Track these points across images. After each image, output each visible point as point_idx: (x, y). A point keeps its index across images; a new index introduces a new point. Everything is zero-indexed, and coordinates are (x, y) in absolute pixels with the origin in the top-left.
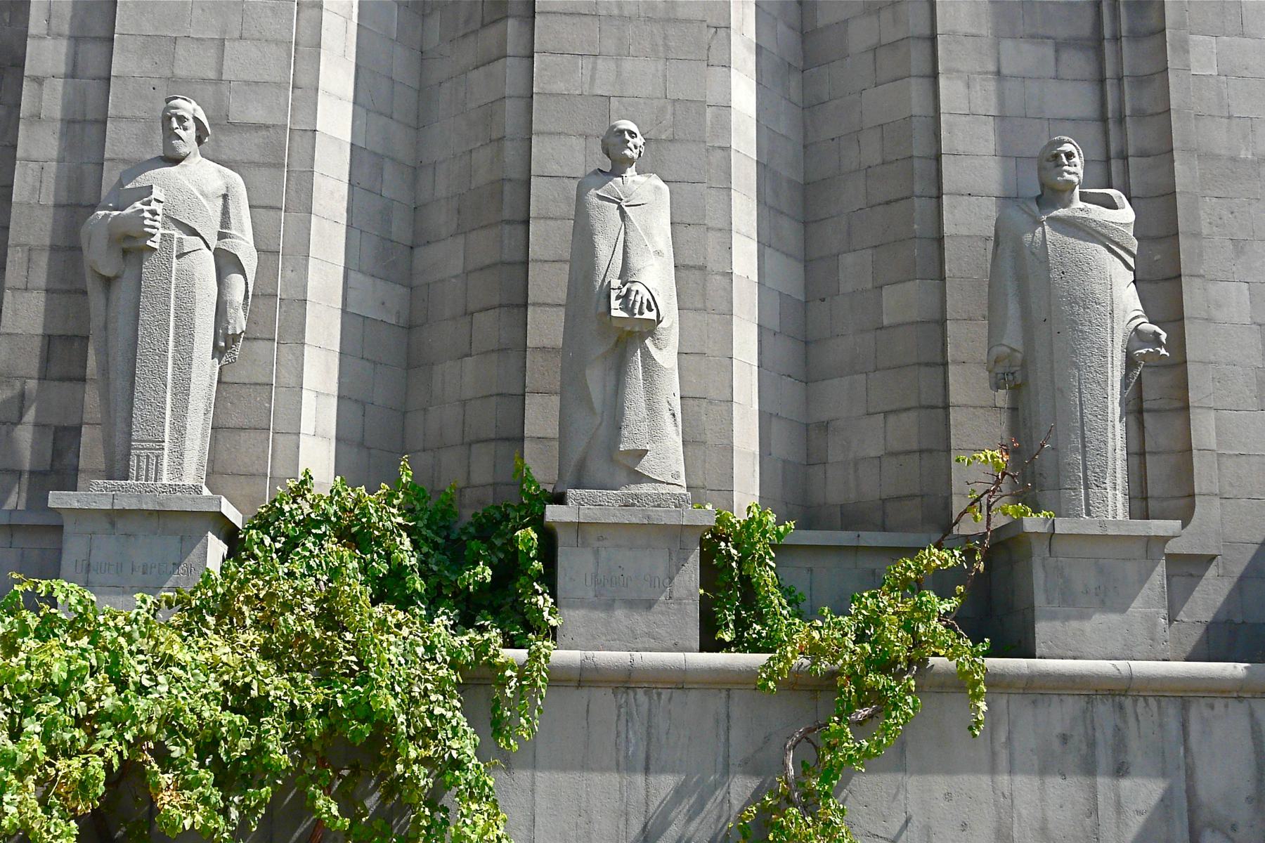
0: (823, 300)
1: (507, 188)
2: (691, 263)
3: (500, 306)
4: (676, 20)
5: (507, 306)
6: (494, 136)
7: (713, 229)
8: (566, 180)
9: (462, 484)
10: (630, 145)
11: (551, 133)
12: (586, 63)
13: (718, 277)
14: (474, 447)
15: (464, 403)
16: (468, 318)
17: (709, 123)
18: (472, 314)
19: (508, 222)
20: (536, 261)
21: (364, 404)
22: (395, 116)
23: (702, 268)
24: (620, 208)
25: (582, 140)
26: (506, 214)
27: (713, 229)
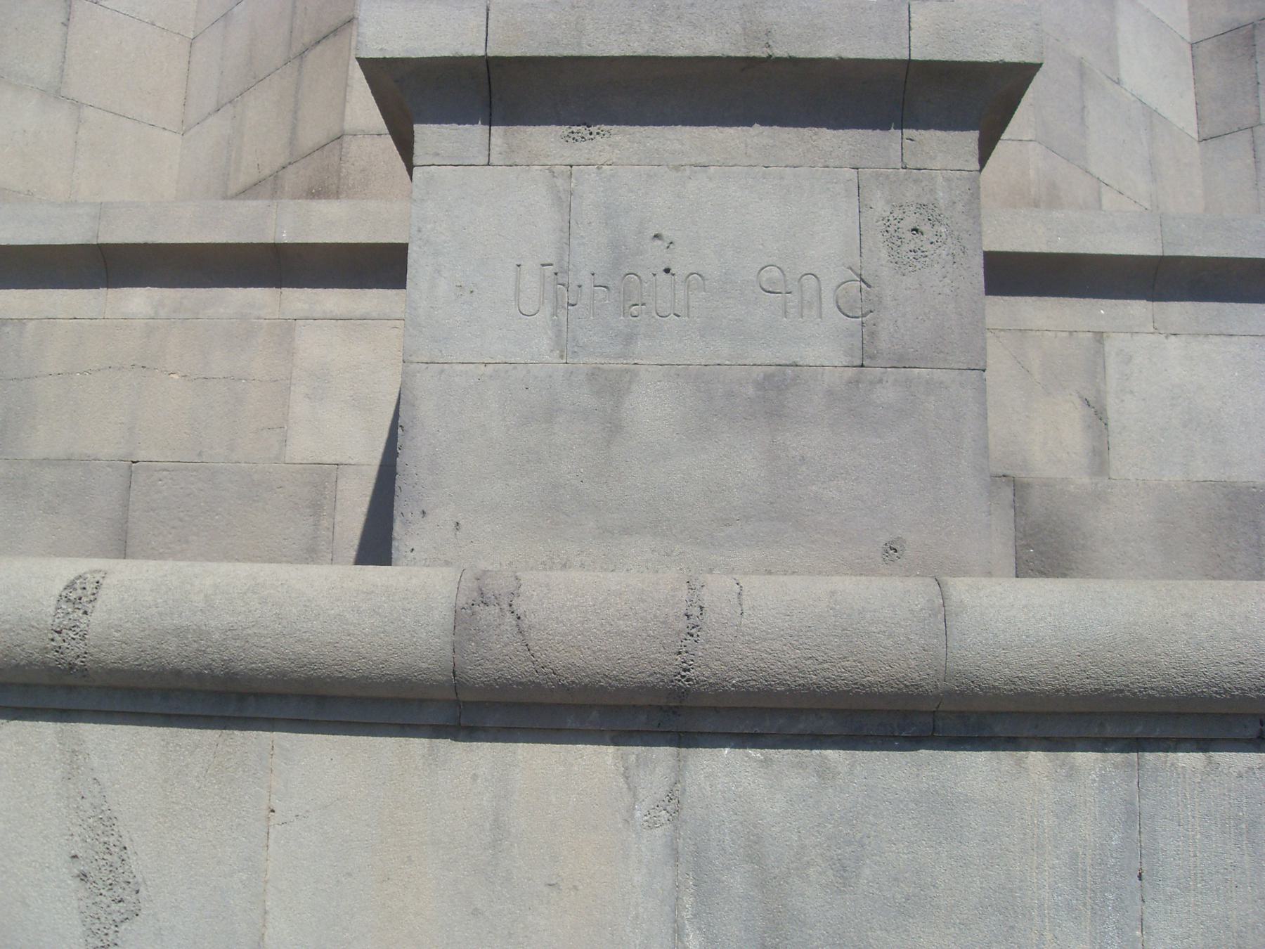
9: (282, 160)
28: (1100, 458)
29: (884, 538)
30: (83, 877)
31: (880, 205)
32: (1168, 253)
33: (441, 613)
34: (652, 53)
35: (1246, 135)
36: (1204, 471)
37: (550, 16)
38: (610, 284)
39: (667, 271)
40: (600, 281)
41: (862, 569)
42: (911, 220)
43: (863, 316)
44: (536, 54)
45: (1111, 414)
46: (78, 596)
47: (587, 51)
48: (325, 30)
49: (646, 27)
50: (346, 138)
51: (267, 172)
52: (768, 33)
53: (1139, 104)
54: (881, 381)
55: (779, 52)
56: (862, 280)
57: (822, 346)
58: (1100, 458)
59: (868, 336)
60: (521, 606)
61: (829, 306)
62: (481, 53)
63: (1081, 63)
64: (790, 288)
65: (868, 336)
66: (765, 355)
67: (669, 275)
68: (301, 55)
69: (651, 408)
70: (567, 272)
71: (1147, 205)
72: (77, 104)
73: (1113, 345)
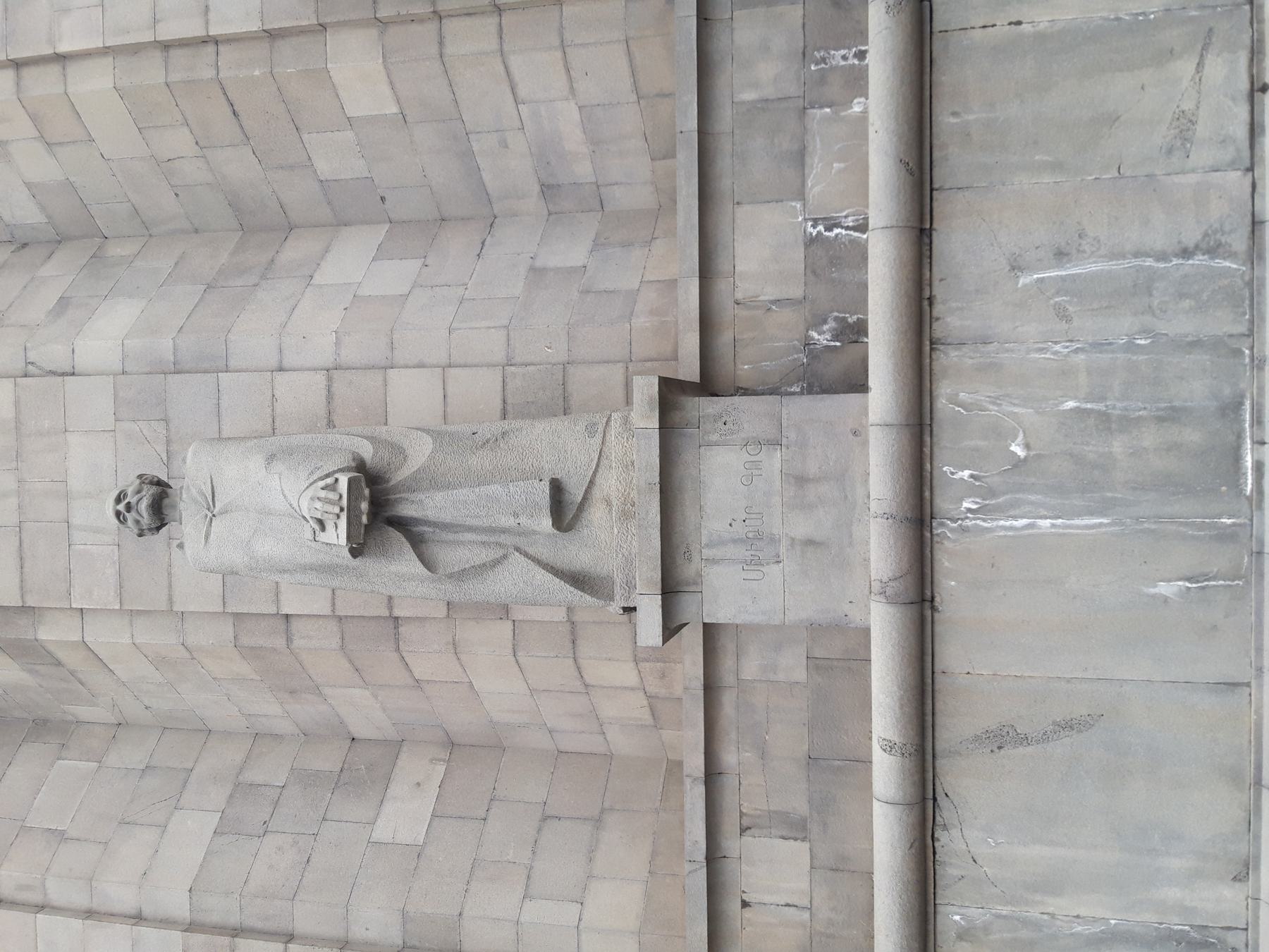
0: (383, 199)
1: (245, 640)
2: (324, 392)
3: (398, 649)
4: (18, 421)
5: (397, 641)
6: (187, 655)
9: (641, 694)
10: (133, 500)
11: (170, 586)
12: (77, 536)
14: (588, 680)
15: (532, 691)
19: (289, 640)
21: (545, 818)
22: (190, 765)
26: (280, 642)
29: (851, 436)
30: (1000, 748)
31: (714, 437)
33: (891, 609)
35: (602, 190)
41: (865, 443)
42: (720, 424)
46: (889, 748)
48: (576, 674)
51: (645, 703)
57: (774, 461)
60: (885, 579)
66: (778, 483)
68: (586, 686)
72: (603, 811)
73: (739, 295)
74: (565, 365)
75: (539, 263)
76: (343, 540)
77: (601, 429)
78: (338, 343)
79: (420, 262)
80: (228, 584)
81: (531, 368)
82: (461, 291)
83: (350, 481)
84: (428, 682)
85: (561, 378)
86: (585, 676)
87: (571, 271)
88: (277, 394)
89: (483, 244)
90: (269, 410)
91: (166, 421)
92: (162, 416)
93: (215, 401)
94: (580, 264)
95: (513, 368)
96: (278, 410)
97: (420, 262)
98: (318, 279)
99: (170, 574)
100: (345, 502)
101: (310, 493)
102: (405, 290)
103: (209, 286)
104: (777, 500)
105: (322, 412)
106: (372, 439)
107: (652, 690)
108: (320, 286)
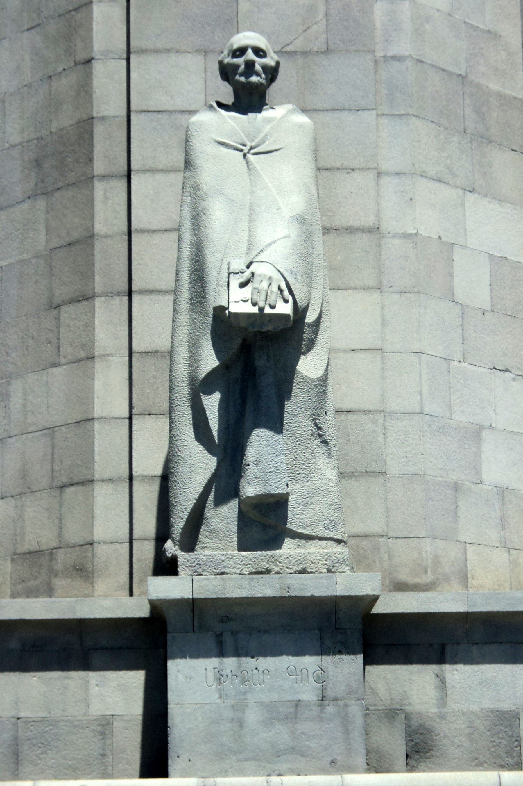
2: (356, 224)
7: (387, 174)
8: (179, 116)
9: (54, 544)
11: (156, 51)
13: (397, 241)
15: (50, 430)
16: (55, 312)
17: (378, 24)
18: (58, 306)
20: (142, 231)
23: (374, 230)
24: (245, 155)
25: (200, 58)
27: (387, 174)
28: (442, 701)
29: (330, 759)
32: (470, 610)
34: (250, 596)
36: (488, 704)
37: (214, 583)
38: (237, 674)
39: (256, 669)
40: (234, 673)
43: (322, 683)
44: (210, 597)
45: (448, 680)
47: (228, 596)
49: (247, 586)
50: (95, 545)
51: (44, 547)
52: (288, 587)
53: (495, 489)
54: (328, 705)
55: (292, 594)
56: (322, 670)
58: (442, 701)
59: (324, 689)
61: (311, 678)
62: (191, 597)
63: (456, 483)
64: (298, 674)
65: (324, 689)
67: (256, 671)
69: (253, 716)
70: (222, 671)
71: (497, 545)
74: (383, 473)
75: (485, 433)
76: (234, 308)
77: (331, 534)
78: (406, 236)
79: (487, 306)
80: (160, 116)
81: (381, 439)
82: (458, 356)
83: (287, 316)
84: (58, 318)
85: (372, 470)
86: (72, 489)
87: (477, 469)
88: (355, 175)
89: (507, 370)
90: (338, 165)
91: (327, 51)
92: (332, 47)
93: (347, 106)
94: (485, 477)
95: (381, 421)
96: (338, 175)
97: (487, 306)
98: (471, 198)
99: (168, 51)
100: (268, 310)
101: (276, 276)
102: (460, 296)
103: (463, 78)
104: (275, 696)
105: (336, 223)
106: (320, 317)
107: (61, 556)
108: (463, 204)
